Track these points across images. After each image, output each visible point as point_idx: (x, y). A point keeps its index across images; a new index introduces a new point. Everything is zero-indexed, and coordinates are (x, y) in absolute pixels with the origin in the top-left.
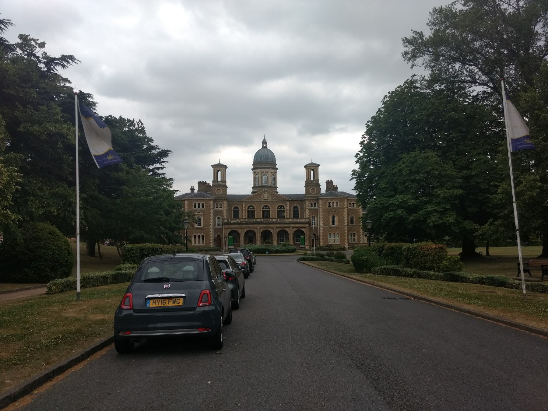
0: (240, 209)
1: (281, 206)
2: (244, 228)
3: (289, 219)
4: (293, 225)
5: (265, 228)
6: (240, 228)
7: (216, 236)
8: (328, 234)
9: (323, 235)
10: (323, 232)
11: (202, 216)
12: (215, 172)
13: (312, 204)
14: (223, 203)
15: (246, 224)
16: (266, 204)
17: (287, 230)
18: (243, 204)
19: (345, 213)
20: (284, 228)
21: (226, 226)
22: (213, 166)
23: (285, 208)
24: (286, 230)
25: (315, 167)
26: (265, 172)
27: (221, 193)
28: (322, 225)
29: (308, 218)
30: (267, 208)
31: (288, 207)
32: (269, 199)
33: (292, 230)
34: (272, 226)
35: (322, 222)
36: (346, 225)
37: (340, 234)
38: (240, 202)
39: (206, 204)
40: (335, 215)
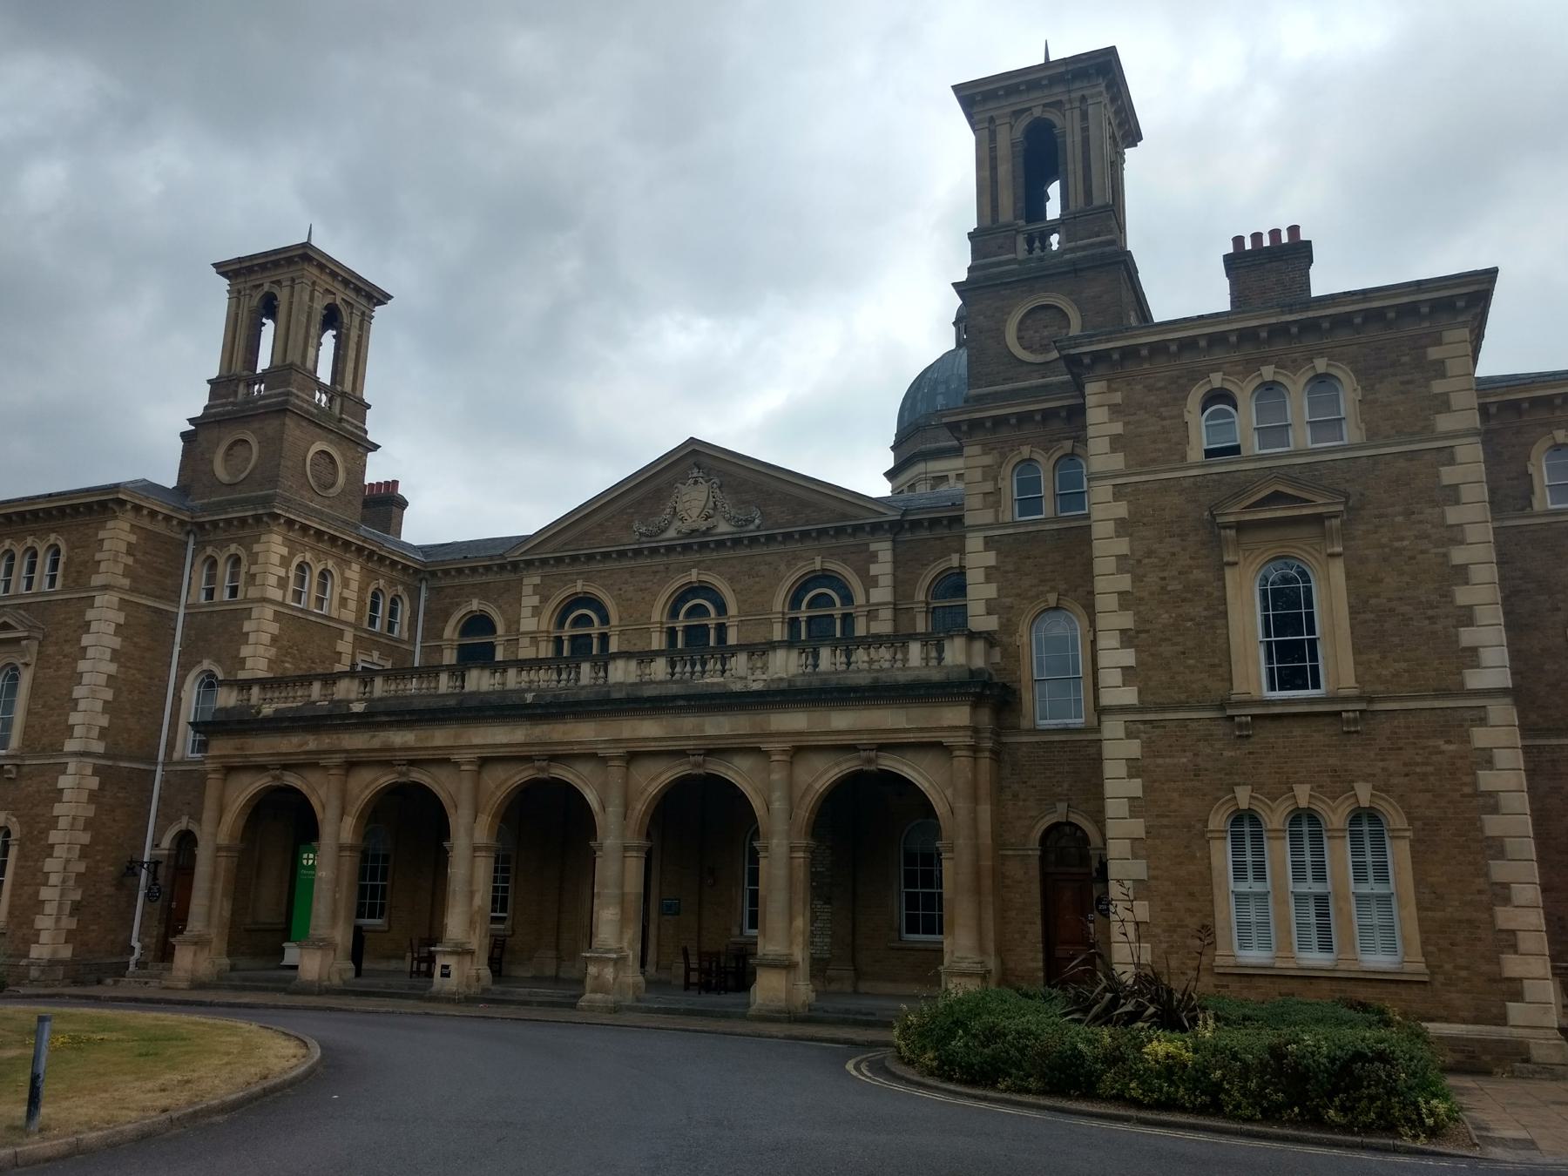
0: (500, 629)
1: (826, 578)
2: (352, 764)
3: (759, 650)
4: (794, 721)
5: (528, 759)
6: (309, 764)
7: (166, 842)
8: (1219, 820)
9: (1137, 827)
10: (1135, 787)
11: (27, 660)
12: (237, 314)
13: (1029, 485)
14: (248, 549)
15: (370, 720)
16: (694, 576)
17: (739, 772)
18: (527, 590)
19: (1453, 515)
20: (710, 752)
21: (223, 747)
22: (234, 271)
23: (859, 599)
24: (731, 776)
25: (1058, 92)
26: (952, 474)
27: (250, 467)
28: (1129, 696)
29: (989, 639)
30: (697, 611)
31: (886, 581)
32: (724, 528)
33: (790, 784)
34: (584, 732)
35: (1128, 657)
36: (1503, 679)
37: (1395, 818)
38: (506, 576)
39: (72, 547)
40: (1305, 551)
